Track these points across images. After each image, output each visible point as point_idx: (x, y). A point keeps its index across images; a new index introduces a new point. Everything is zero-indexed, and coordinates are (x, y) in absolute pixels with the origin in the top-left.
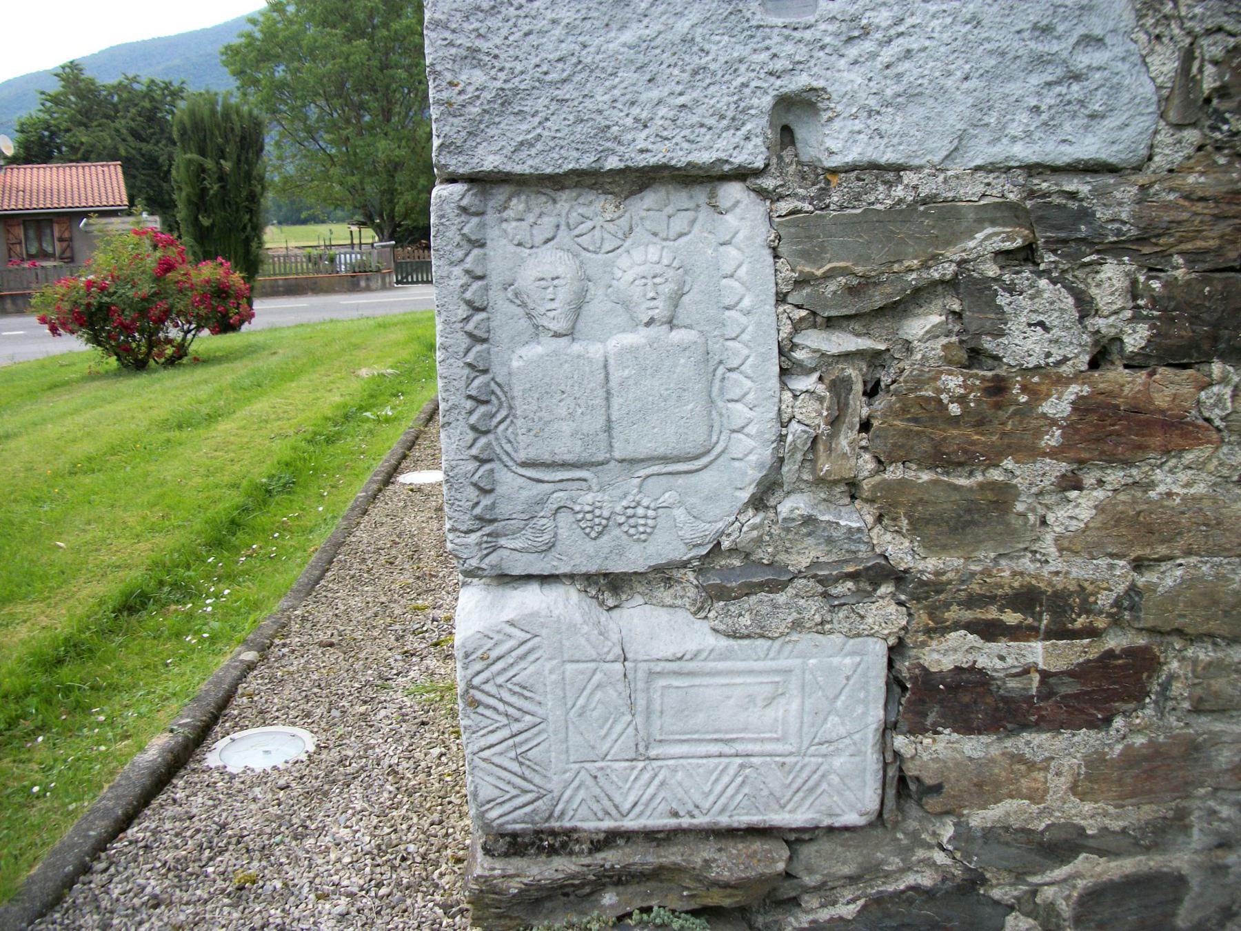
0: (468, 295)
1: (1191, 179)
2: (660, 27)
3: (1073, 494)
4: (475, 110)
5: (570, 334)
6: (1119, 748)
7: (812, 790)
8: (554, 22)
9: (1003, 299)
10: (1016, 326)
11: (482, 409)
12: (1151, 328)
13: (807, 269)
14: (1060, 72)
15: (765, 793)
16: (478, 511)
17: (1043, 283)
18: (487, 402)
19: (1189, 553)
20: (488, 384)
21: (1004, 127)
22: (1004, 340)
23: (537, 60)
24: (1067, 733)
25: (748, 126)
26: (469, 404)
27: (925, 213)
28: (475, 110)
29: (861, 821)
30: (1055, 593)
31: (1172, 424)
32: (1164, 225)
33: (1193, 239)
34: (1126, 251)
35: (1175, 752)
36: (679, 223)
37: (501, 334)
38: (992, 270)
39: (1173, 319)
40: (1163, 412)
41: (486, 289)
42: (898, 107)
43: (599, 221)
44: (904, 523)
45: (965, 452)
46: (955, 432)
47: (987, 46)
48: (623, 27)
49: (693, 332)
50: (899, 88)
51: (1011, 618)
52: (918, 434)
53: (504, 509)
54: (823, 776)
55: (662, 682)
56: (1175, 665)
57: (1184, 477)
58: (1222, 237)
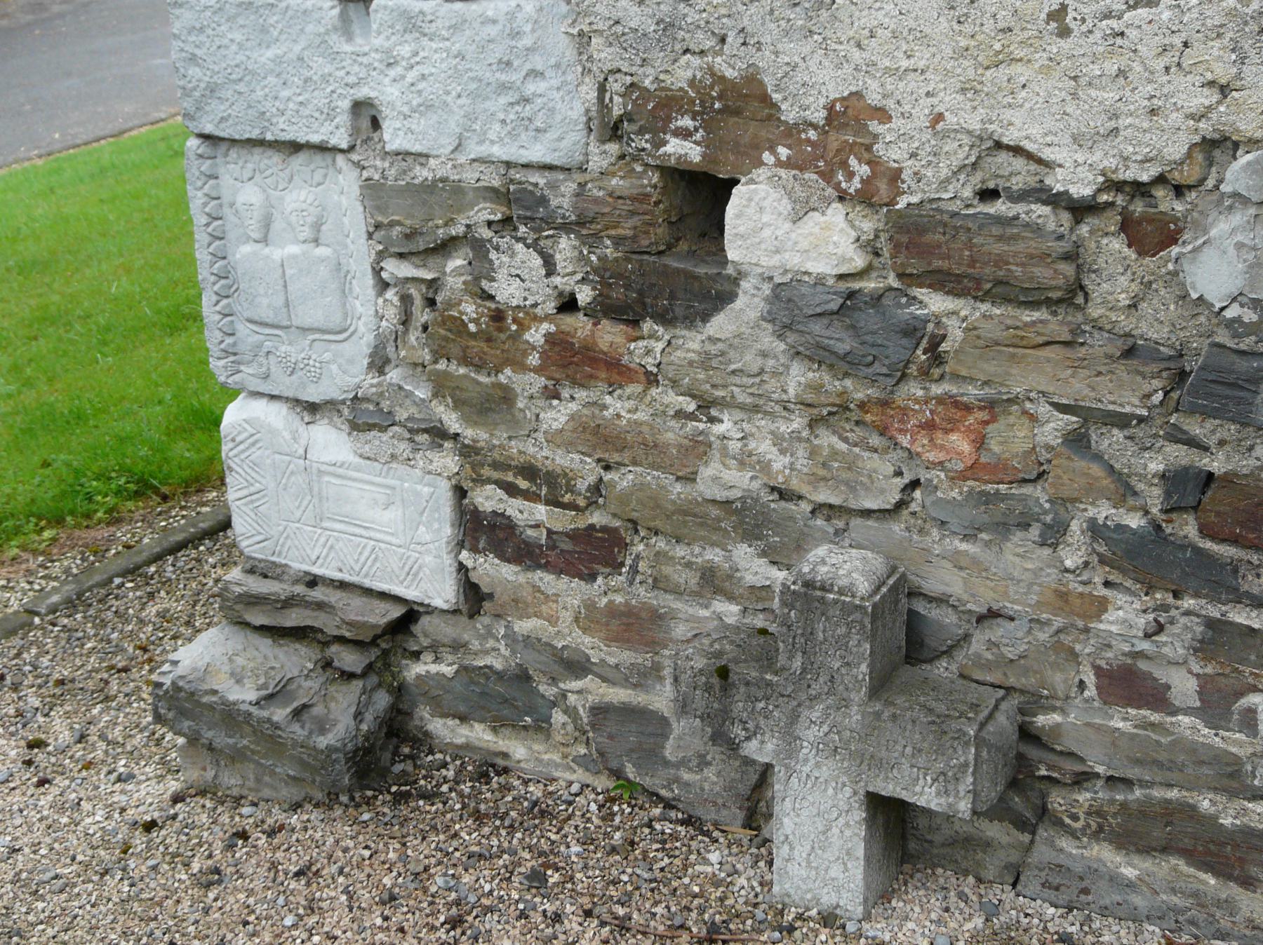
0: (207, 210)
1: (614, 182)
2: (285, 49)
3: (555, 402)
4: (197, 94)
5: (264, 240)
6: (605, 600)
7: (416, 575)
8: (232, 40)
9: (493, 255)
10: (501, 275)
11: (223, 282)
12: (594, 289)
13: (380, 219)
14: (517, 96)
15: (389, 569)
16: (222, 346)
17: (519, 247)
18: (227, 278)
19: (635, 463)
20: (226, 266)
21: (485, 133)
22: (495, 284)
23: (224, 65)
24: (565, 579)
25: (337, 120)
26: (213, 278)
27: (443, 189)
28: (197, 94)
29: (445, 607)
30: (548, 472)
31: (612, 364)
32: (591, 215)
33: (615, 227)
34: (573, 231)
35: (643, 615)
36: (318, 176)
37: (232, 235)
38: (486, 233)
39: (610, 285)
40: (605, 354)
41: (221, 206)
42: (421, 114)
43: (275, 170)
44: (449, 400)
45: (480, 358)
46: (474, 343)
47: (470, 74)
48: (268, 47)
49: (329, 250)
50: (420, 100)
51: (523, 484)
52: (453, 340)
53: (241, 348)
54: (420, 567)
55: (326, 478)
56: (641, 547)
57: (630, 404)
58: (635, 228)
